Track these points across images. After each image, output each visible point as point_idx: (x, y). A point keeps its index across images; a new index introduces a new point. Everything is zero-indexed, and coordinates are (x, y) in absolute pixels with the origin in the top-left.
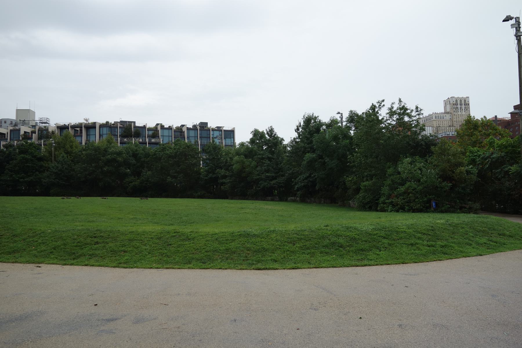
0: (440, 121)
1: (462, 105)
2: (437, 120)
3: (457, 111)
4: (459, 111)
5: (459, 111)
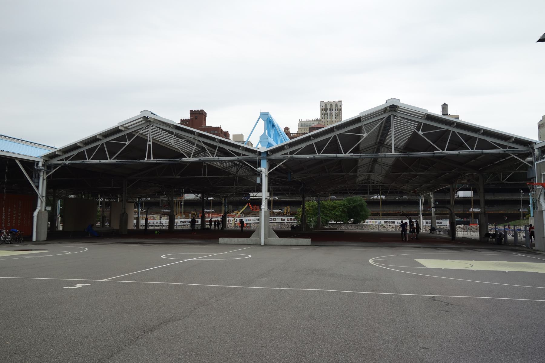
0: (305, 130)
1: (332, 110)
2: (302, 128)
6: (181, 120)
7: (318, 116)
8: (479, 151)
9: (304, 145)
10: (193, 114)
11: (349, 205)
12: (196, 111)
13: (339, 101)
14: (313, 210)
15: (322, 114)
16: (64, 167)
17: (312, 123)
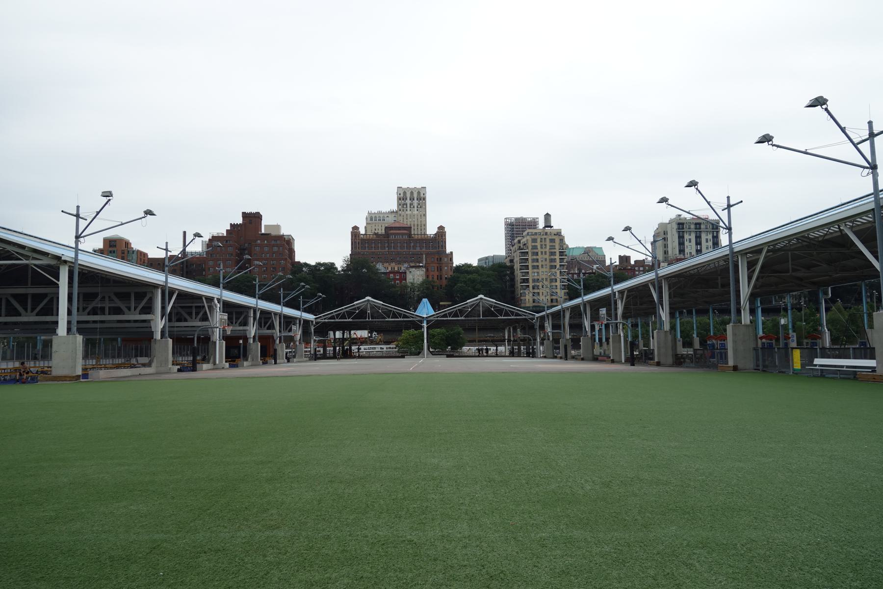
1: (414, 199)
2: (373, 223)
3: (405, 209)
4: (409, 209)
5: (409, 209)
6: (231, 224)
7: (395, 207)
8: (516, 317)
9: (443, 314)
10: (246, 217)
11: (447, 333)
12: (251, 213)
13: (422, 187)
14: (414, 338)
15: (399, 204)
16: (324, 323)
17: (386, 216)
